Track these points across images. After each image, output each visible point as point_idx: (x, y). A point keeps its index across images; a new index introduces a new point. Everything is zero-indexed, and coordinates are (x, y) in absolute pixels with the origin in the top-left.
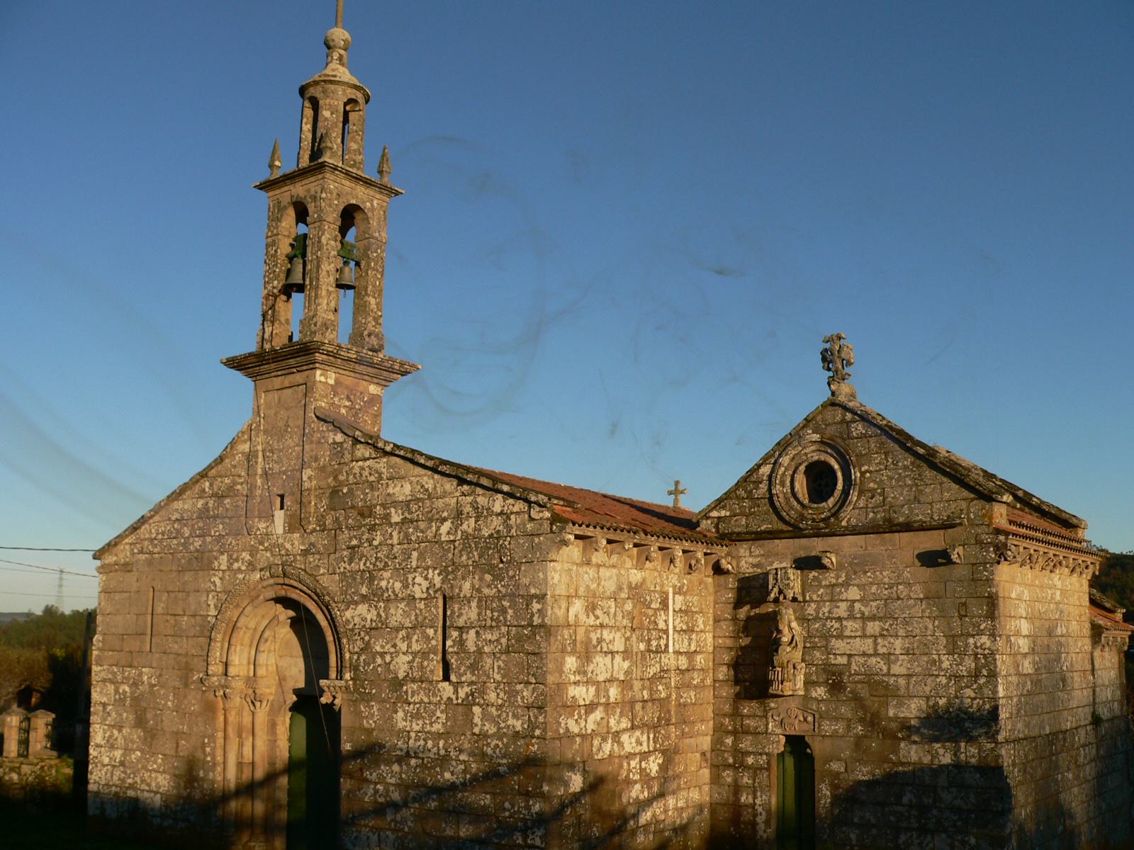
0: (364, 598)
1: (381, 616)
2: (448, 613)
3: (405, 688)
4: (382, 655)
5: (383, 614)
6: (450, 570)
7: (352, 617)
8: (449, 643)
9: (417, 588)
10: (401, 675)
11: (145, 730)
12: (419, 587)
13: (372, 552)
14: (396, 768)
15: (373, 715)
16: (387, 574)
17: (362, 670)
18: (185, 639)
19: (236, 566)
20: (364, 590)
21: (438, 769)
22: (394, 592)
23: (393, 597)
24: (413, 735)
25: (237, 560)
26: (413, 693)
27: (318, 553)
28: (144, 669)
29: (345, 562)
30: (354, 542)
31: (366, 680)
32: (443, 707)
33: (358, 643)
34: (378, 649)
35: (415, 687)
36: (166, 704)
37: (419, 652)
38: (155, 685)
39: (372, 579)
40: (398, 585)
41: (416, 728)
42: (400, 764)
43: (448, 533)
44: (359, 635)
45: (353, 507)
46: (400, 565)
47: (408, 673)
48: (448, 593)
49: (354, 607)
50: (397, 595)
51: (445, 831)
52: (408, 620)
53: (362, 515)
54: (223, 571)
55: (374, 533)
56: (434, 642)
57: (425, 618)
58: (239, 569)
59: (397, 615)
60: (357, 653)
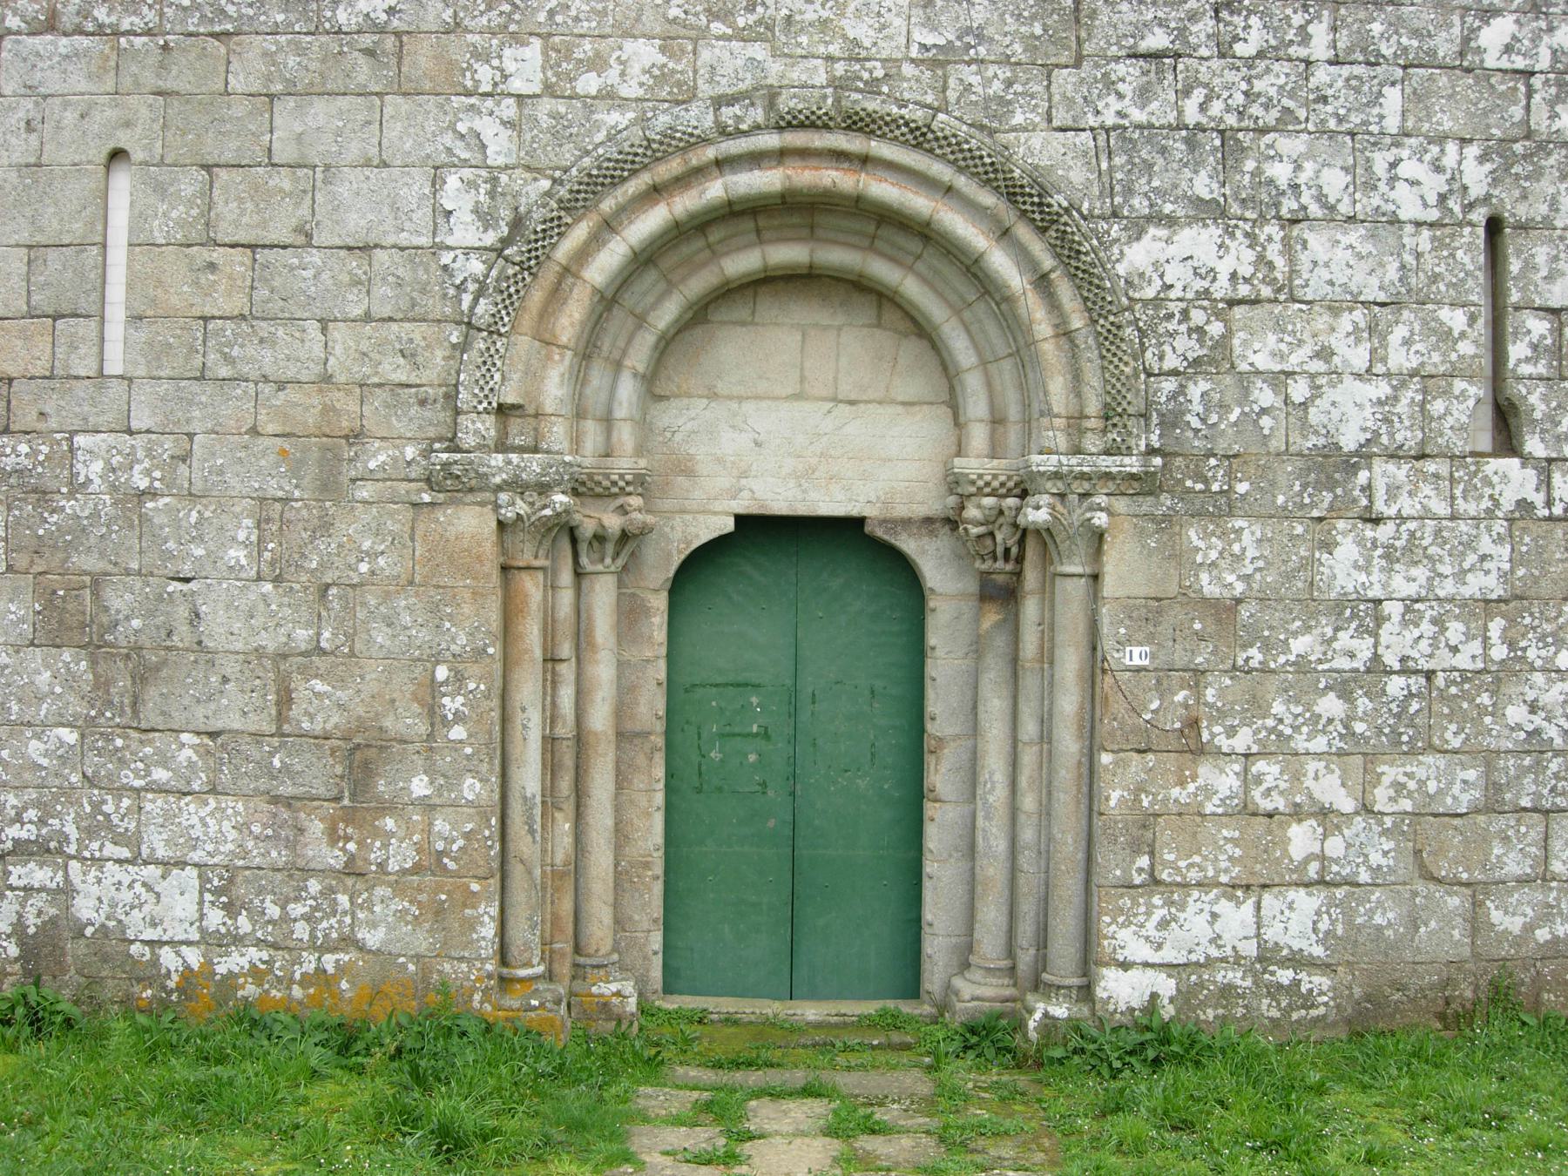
1: (1271, 266)
2: (1515, 266)
3: (1363, 477)
4: (1280, 379)
5: (1280, 262)
6: (1517, 151)
7: (1156, 264)
8: (1517, 351)
9: (1402, 191)
10: (1350, 440)
11: (96, 649)
12: (1414, 190)
13: (1231, 76)
14: (1330, 705)
15: (1238, 558)
16: (1291, 145)
18: (313, 328)
19: (589, 83)
20: (1204, 185)
21: (1485, 699)
22: (1320, 198)
23: (1315, 210)
24: (1393, 609)
25: (597, 63)
26: (1393, 492)
27: (1005, 60)
28: (80, 440)
29: (1120, 96)
30: (1157, 40)
31: (1211, 454)
32: (1500, 527)
33: (1182, 343)
34: (1263, 361)
35: (1401, 472)
36: (213, 558)
37: (1413, 373)
38: (152, 494)
39: (1230, 148)
40: (1335, 181)
41: (1411, 590)
42: (1346, 695)
43: (1508, 49)
44: (1185, 315)
46: (1340, 120)
47: (1377, 434)
48: (1515, 210)
49: (1163, 233)
50: (1332, 208)
51: (1501, 864)
52: (1374, 281)
54: (520, 98)
56: (1466, 348)
57: (1435, 278)
58: (607, 95)
59: (1332, 258)
60: (1174, 373)
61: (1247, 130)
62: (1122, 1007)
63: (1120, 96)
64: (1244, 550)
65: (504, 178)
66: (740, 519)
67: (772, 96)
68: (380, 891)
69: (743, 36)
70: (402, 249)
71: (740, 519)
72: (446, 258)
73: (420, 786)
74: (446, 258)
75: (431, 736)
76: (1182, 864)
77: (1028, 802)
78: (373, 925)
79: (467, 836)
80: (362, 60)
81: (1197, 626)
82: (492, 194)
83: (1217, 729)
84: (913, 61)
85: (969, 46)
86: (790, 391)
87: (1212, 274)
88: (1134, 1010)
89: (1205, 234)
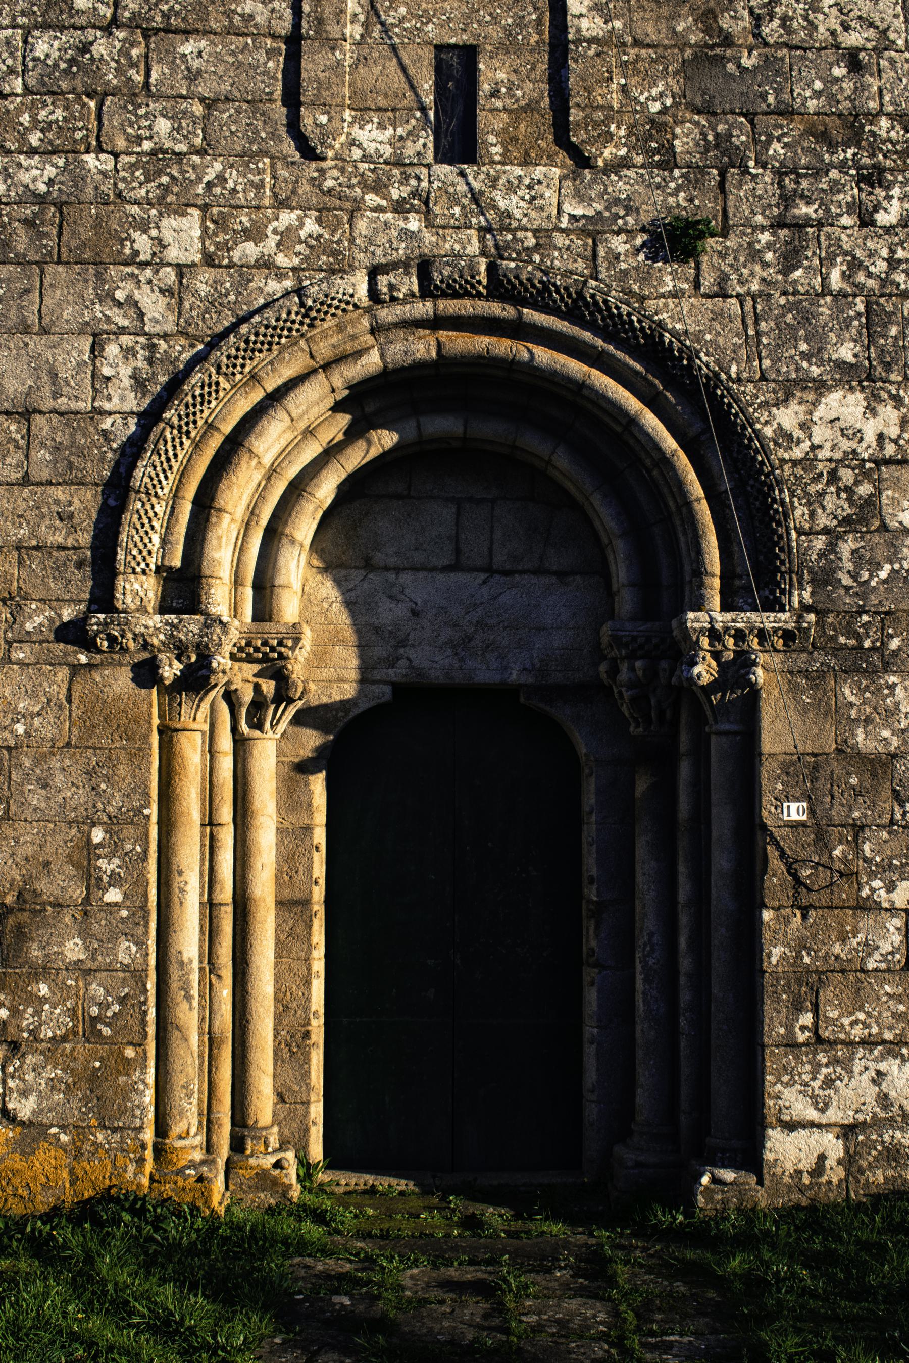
0: (850, 375)
17: (846, 581)
19: (249, 250)
20: (846, 352)
25: (254, 234)
29: (765, 265)
31: (862, 611)
44: (833, 477)
45: (786, 111)
53: (824, 137)
55: (880, 193)
58: (266, 264)
60: (826, 531)
61: (890, 296)
62: (790, 1168)
63: (765, 265)
64: (897, 704)
65: (163, 345)
66: (395, 686)
67: (424, 267)
68: (30, 1059)
69: (400, 207)
70: (61, 414)
71: (396, 687)
72: (107, 423)
73: (74, 949)
74: (107, 423)
75: (87, 900)
76: (846, 1021)
77: (685, 964)
78: (24, 1094)
79: (122, 1001)
80: (21, 231)
81: (854, 781)
82: (150, 361)
83: (877, 884)
84: (562, 231)
85: (617, 216)
86: (446, 562)
87: (858, 436)
88: (799, 1172)
89: (851, 398)
